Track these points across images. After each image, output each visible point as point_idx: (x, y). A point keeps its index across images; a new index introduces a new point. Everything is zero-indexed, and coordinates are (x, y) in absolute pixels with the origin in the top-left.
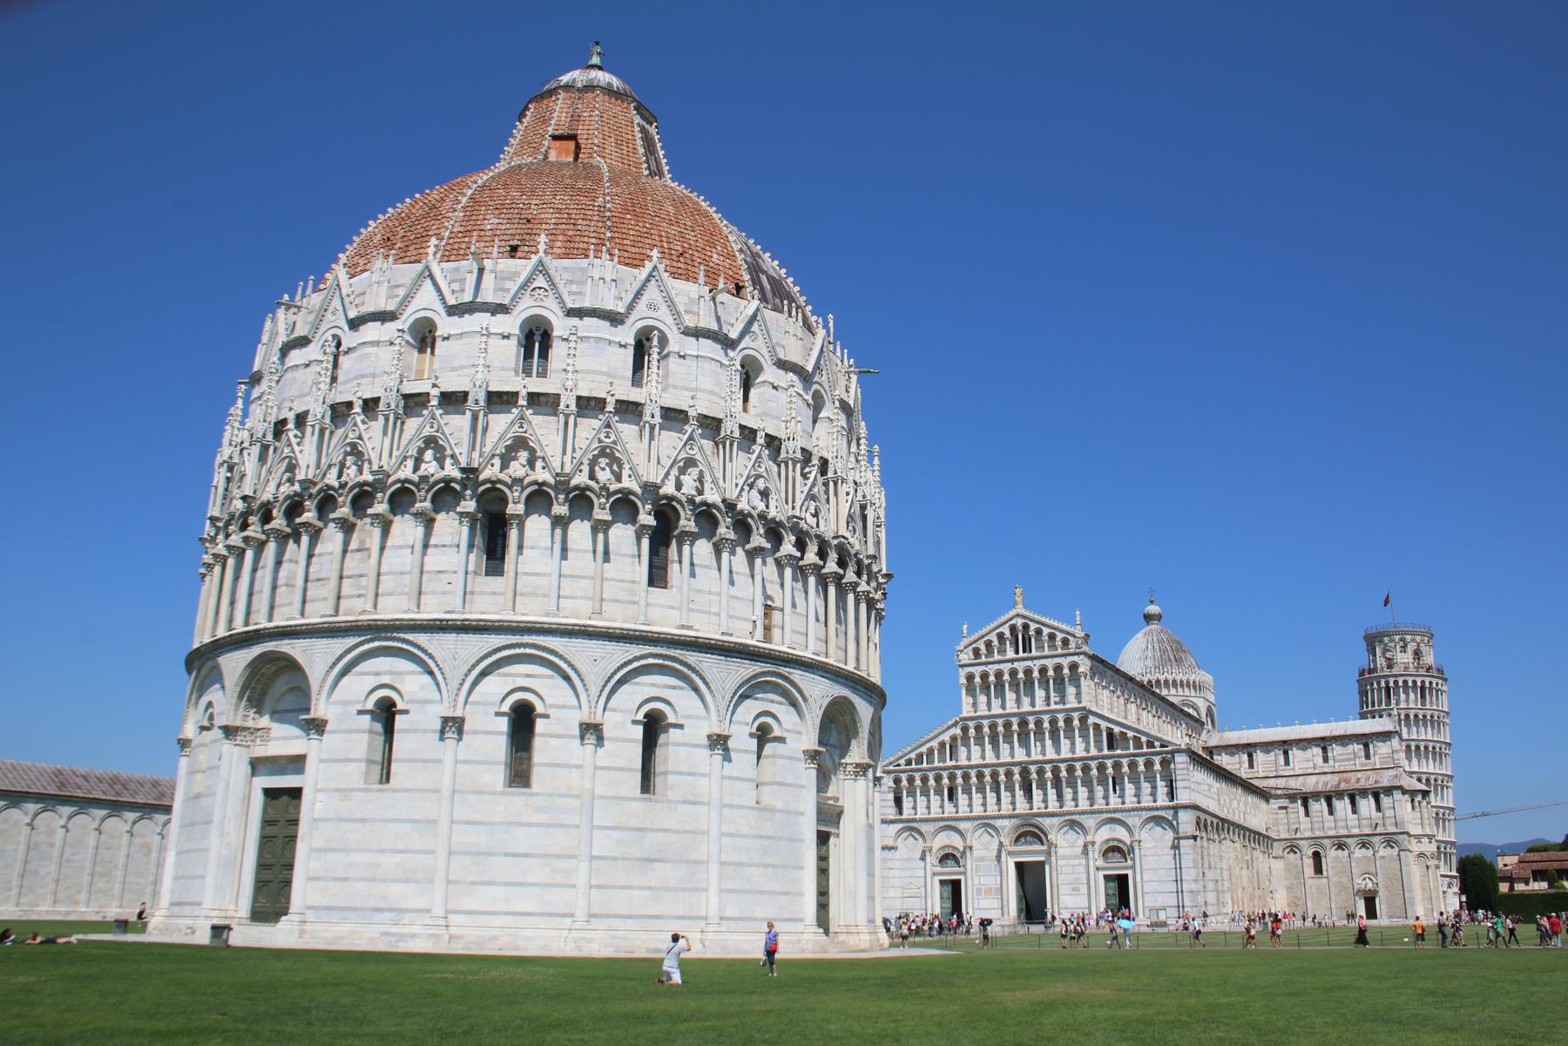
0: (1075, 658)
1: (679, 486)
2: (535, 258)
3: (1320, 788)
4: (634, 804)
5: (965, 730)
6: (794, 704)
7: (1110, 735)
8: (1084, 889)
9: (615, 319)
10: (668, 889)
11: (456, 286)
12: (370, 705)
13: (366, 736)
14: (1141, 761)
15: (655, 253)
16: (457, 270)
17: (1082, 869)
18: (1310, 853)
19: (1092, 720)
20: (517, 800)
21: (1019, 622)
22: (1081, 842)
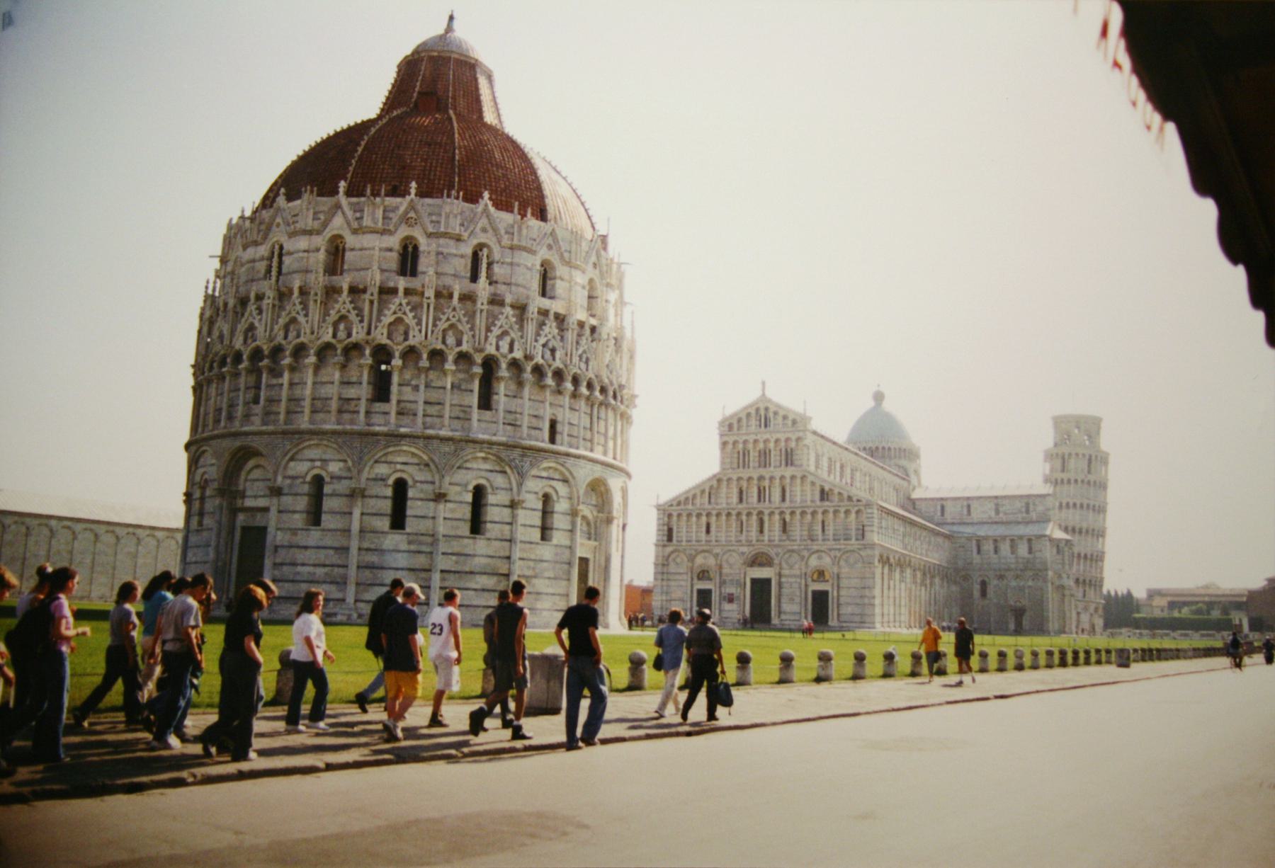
1: (498, 348)
2: (408, 198)
3: (990, 533)
4: (466, 541)
5: (719, 481)
6: (565, 481)
8: (797, 600)
9: (458, 239)
10: (483, 590)
11: (358, 215)
12: (308, 478)
13: (306, 498)
15: (486, 195)
16: (358, 203)
17: (796, 585)
19: (810, 478)
20: (394, 540)
21: (762, 406)
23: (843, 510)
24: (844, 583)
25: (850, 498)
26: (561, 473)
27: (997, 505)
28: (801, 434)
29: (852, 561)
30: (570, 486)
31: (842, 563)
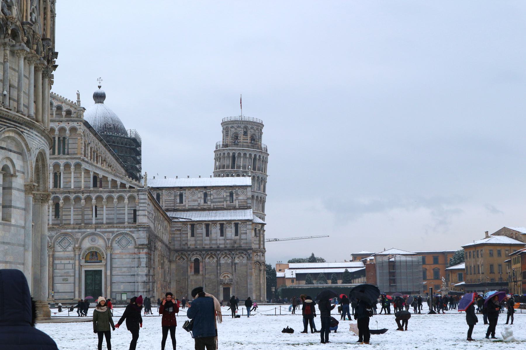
0: (75, 124)
6: (20, 153)
7: (95, 178)
8: (71, 279)
14: (115, 196)
17: (70, 266)
18: (193, 259)
19: (84, 166)
22: (70, 248)
23: (115, 196)
24: (117, 263)
25: (123, 186)
26: (18, 144)
27: (206, 195)
28: (75, 124)
29: (124, 242)
30: (24, 160)
31: (115, 245)
